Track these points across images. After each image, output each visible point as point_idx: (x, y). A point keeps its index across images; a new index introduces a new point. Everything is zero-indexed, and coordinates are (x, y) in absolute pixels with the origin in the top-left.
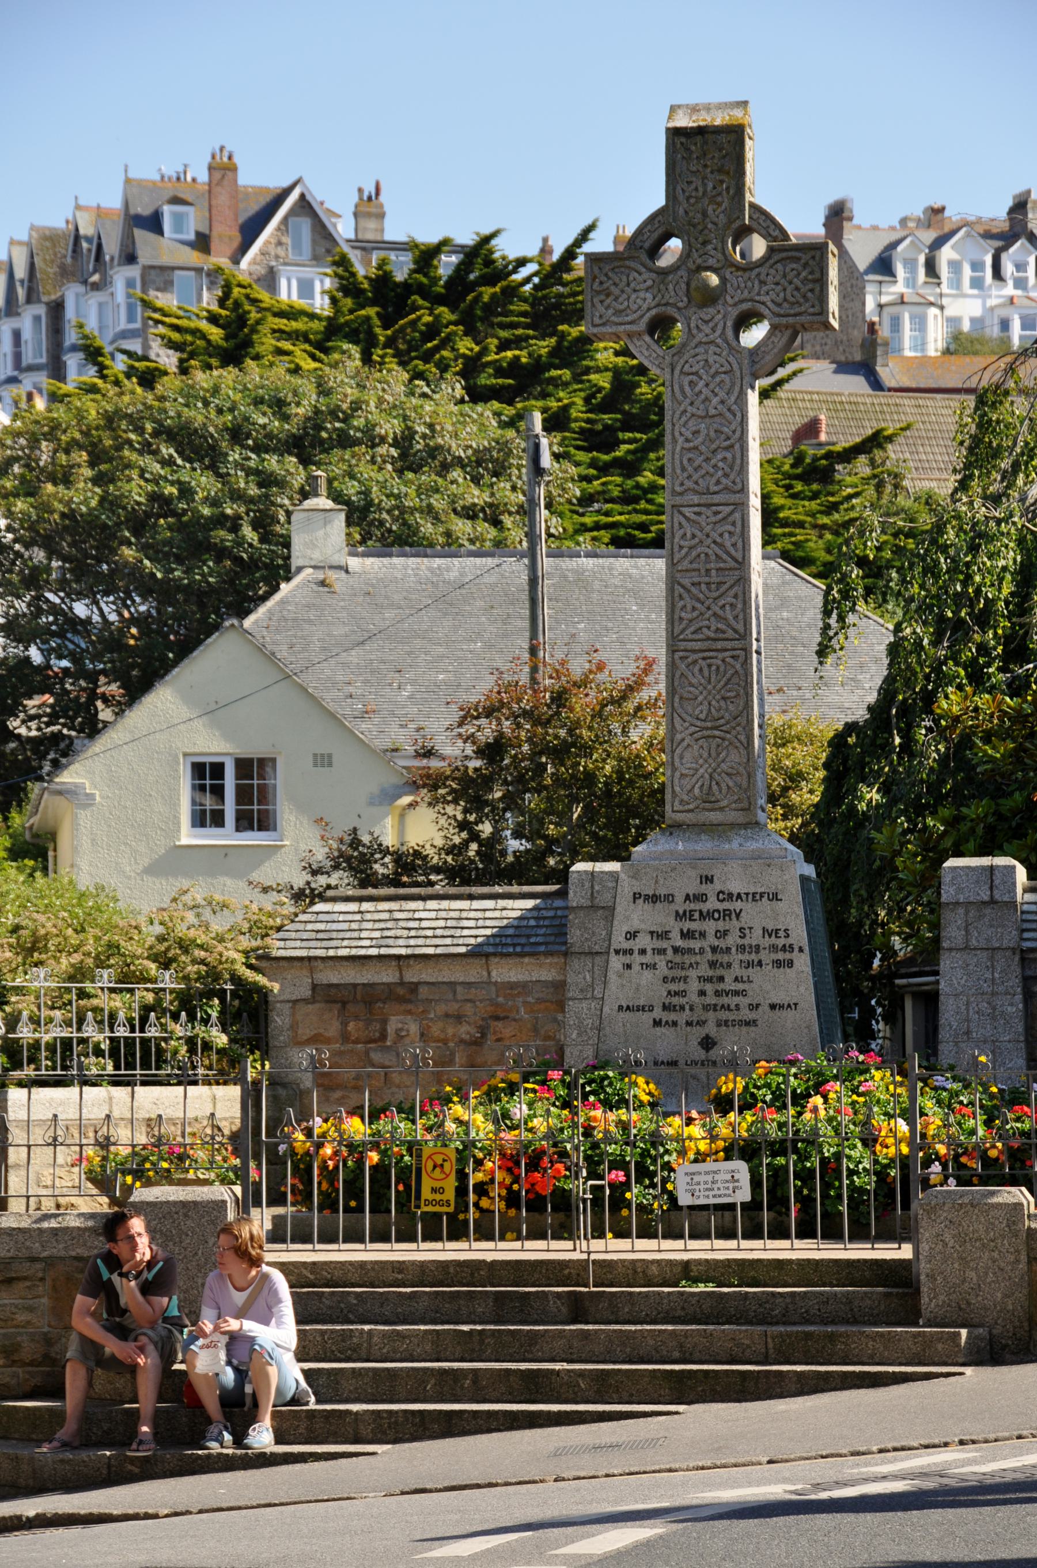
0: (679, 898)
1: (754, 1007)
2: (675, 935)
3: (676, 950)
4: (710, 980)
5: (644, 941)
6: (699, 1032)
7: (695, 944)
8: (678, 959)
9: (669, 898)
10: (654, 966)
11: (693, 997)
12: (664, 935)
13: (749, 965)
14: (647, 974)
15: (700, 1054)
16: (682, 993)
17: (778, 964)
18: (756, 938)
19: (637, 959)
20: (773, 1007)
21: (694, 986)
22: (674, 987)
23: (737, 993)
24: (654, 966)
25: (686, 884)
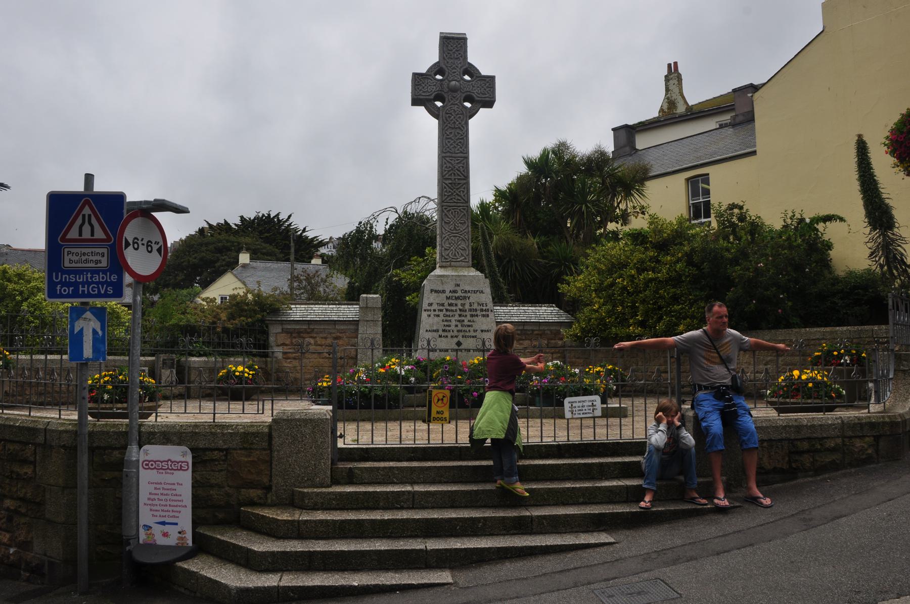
0: (448, 291)
1: (475, 331)
2: (446, 304)
3: (447, 310)
4: (459, 321)
5: (435, 307)
6: (456, 340)
7: (454, 308)
8: (448, 313)
9: (444, 292)
10: (438, 316)
11: (453, 327)
12: (443, 305)
13: (472, 316)
14: (436, 318)
15: (456, 347)
16: (449, 326)
17: (483, 316)
18: (475, 306)
19: (432, 313)
20: (482, 331)
21: (453, 323)
22: (446, 323)
23: (469, 326)
24: (438, 316)
25: (448, 287)
